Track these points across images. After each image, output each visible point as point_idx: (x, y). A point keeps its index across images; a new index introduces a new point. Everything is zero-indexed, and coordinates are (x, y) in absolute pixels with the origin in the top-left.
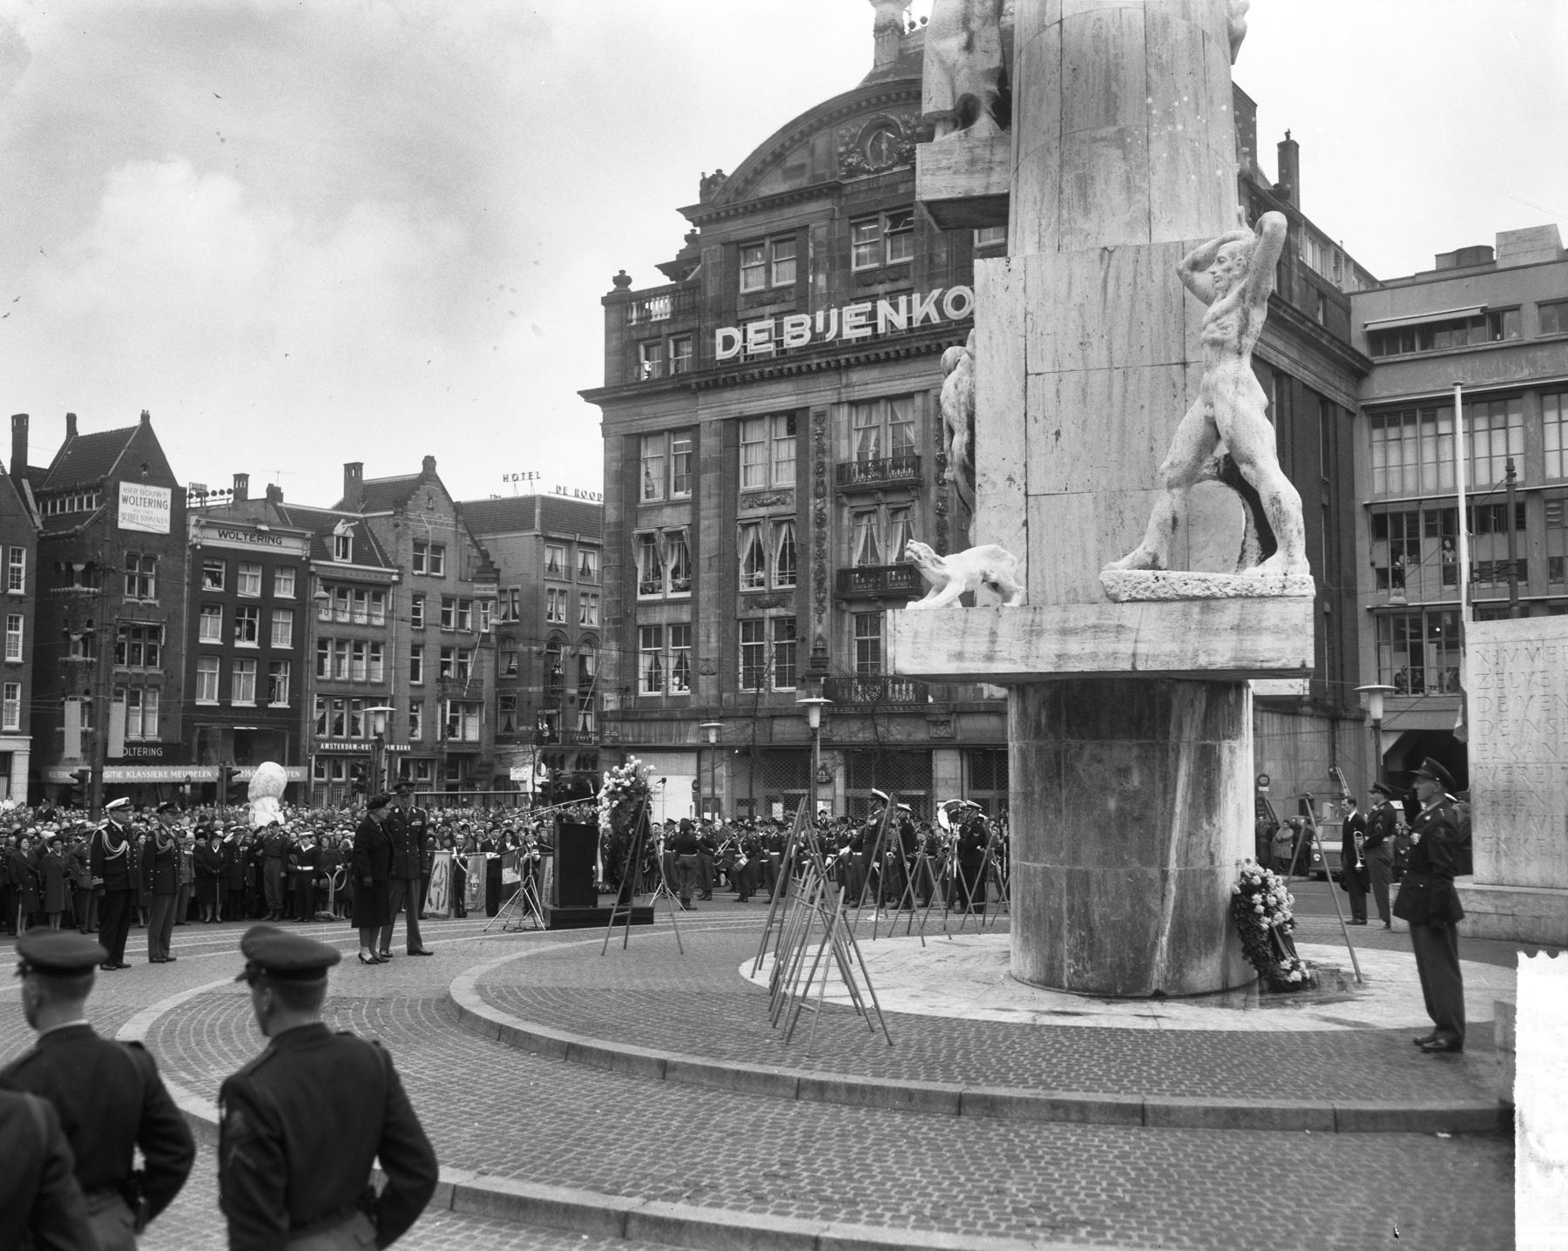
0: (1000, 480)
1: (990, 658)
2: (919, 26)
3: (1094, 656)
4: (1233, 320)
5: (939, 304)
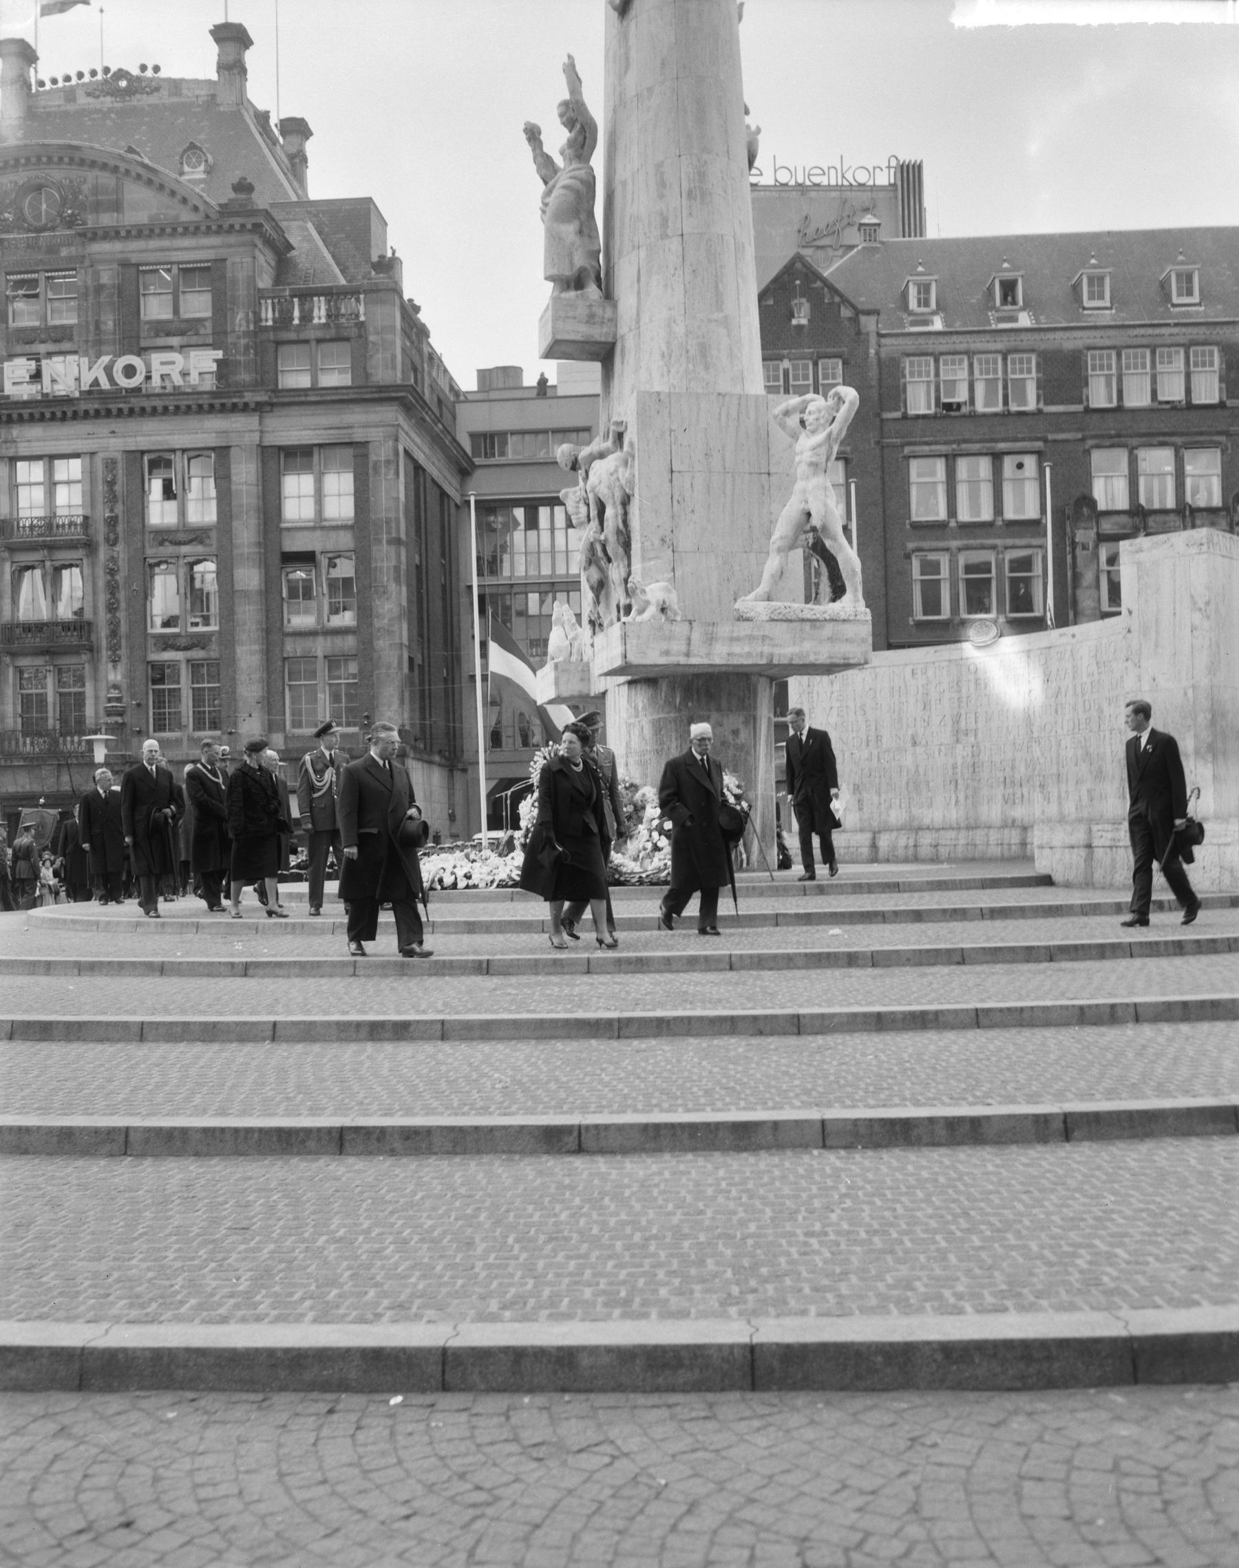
0: (657, 542)
1: (688, 655)
2: (48, 86)
3: (749, 654)
4: (823, 450)
5: (108, 370)
